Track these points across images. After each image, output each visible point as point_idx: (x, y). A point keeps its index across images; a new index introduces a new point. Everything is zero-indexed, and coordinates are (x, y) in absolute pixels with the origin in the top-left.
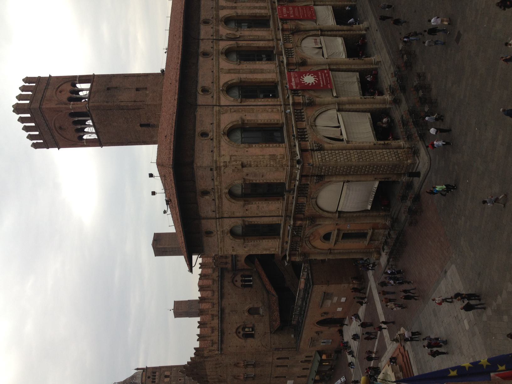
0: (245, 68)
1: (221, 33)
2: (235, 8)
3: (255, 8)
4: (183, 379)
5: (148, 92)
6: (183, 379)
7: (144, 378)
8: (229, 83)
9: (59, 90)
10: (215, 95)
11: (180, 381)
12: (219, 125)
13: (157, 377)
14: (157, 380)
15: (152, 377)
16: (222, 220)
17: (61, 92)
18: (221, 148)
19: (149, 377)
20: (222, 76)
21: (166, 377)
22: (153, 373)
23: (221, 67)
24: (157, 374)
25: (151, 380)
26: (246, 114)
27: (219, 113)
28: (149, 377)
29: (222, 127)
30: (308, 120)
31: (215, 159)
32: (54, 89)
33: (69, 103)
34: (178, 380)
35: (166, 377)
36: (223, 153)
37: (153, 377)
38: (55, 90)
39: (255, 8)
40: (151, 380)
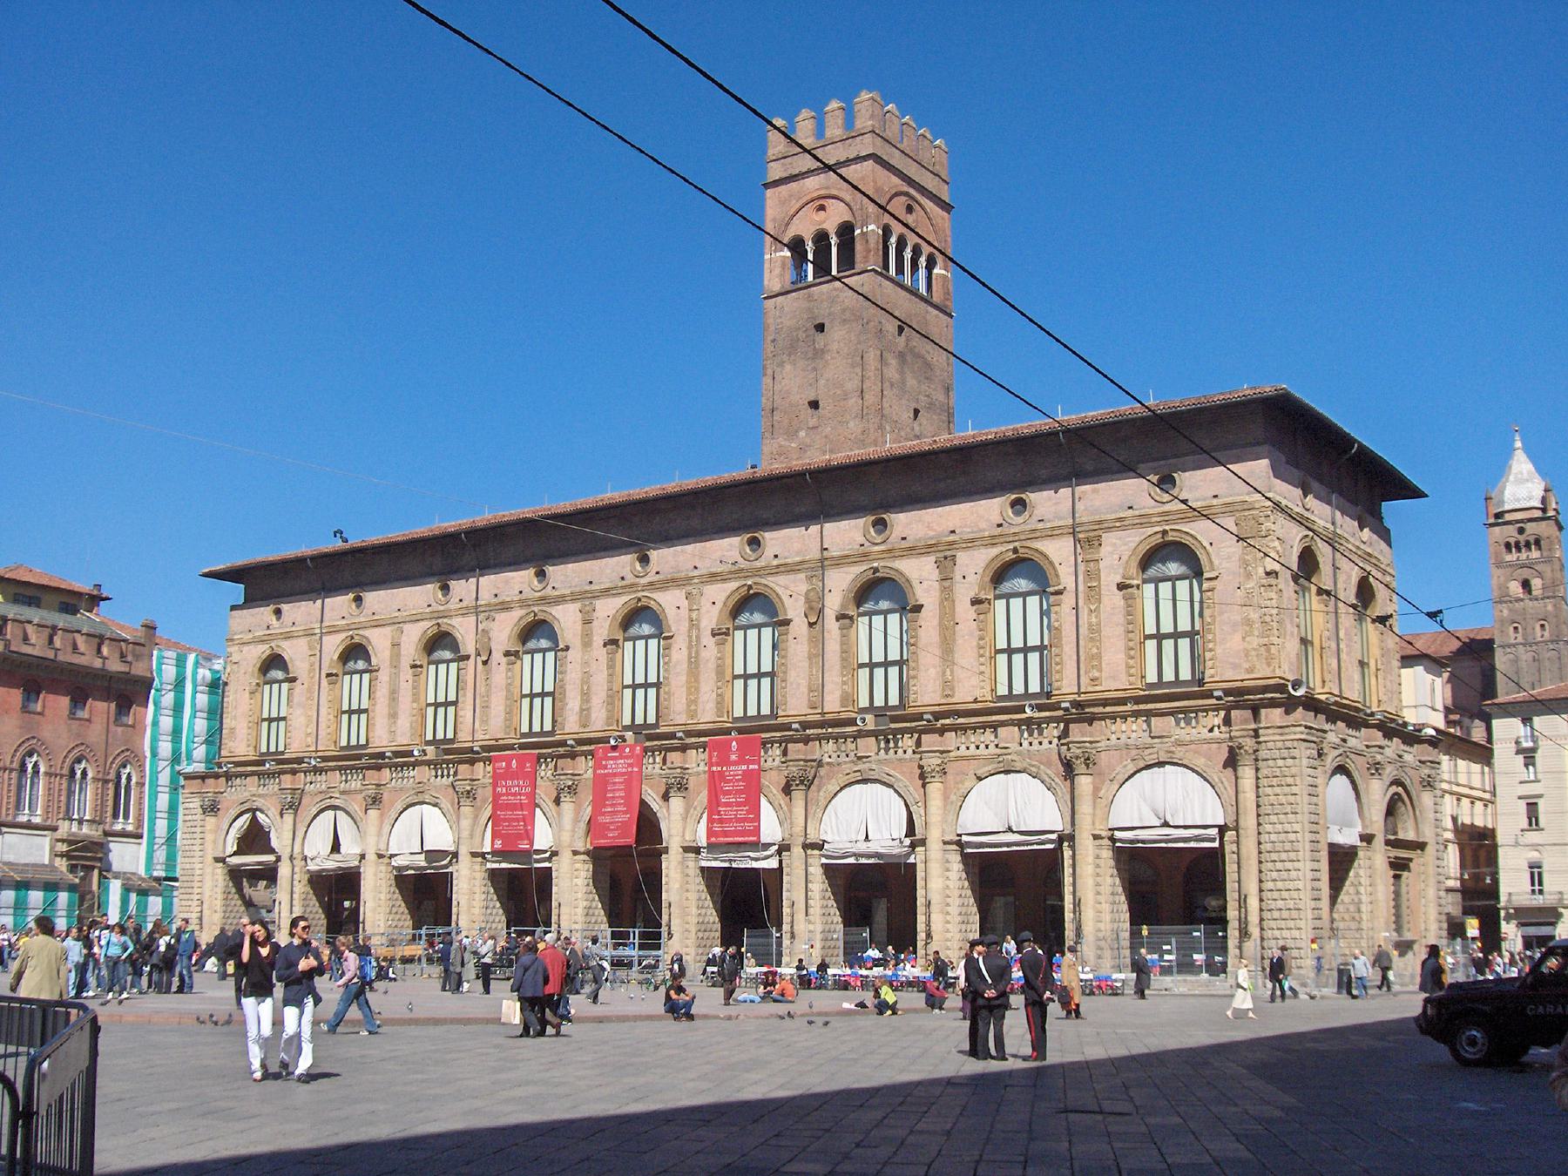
0: (402, 678)
1: (501, 617)
2: (587, 643)
3: (586, 696)
4: (1520, 639)
5: (802, 434)
6: (1520, 639)
7: (1519, 516)
8: (369, 648)
9: (821, 202)
10: (344, 622)
11: (1511, 629)
12: (288, 636)
13: (1524, 555)
14: (1513, 557)
15: (1522, 538)
16: (948, 686)
17: (822, 208)
18: (251, 647)
19: (1521, 531)
20: (387, 631)
21: (1526, 585)
22: (1537, 542)
23: (406, 627)
24: (1535, 554)
25: (1512, 541)
26: (306, 686)
27: (309, 633)
28: (1521, 531)
29: (285, 644)
30: (259, 796)
31: (235, 637)
32: (827, 188)
33: (775, 252)
34: (1516, 625)
35: (1526, 585)
36: (246, 648)
37: (1522, 544)
38: (823, 192)
39: (586, 696)
40: (1512, 541)
